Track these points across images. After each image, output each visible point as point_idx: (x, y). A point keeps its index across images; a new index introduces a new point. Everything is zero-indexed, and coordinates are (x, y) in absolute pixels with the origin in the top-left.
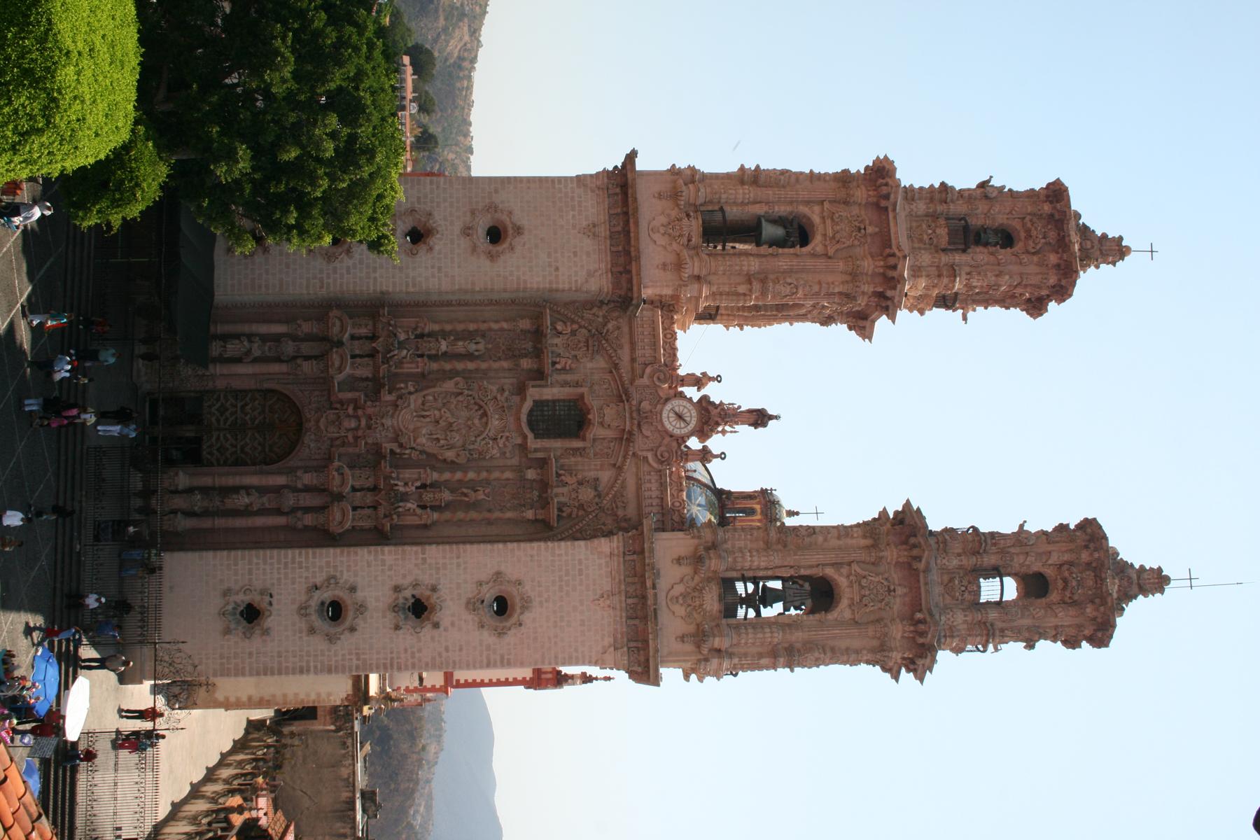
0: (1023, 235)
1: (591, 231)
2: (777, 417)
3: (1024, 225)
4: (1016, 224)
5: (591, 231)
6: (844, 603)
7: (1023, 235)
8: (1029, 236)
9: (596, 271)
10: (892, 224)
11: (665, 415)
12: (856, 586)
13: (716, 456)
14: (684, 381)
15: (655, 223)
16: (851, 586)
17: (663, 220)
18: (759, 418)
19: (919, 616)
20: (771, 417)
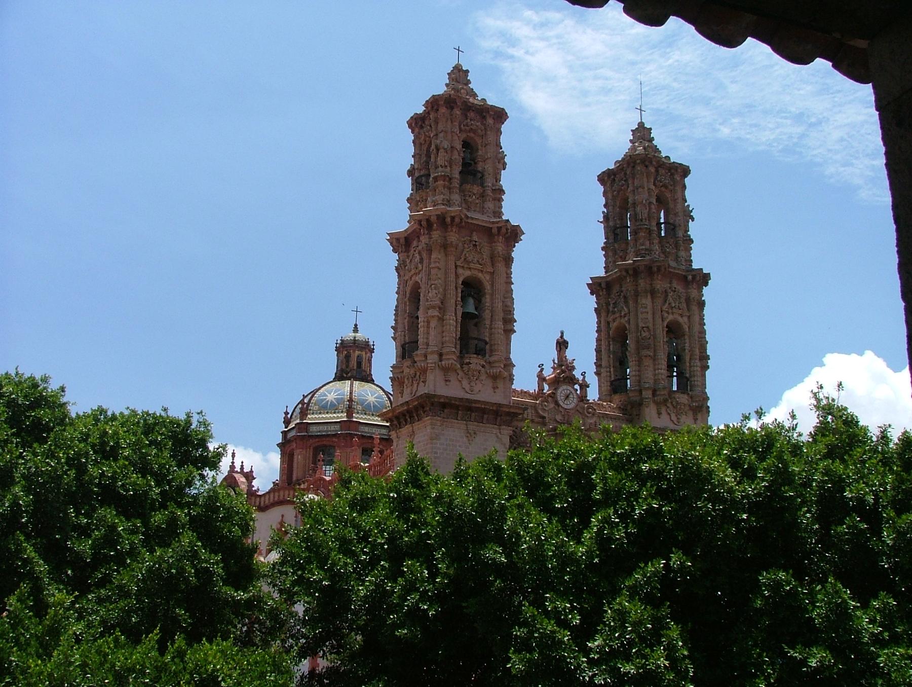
0: (472, 135)
1: (470, 435)
2: (562, 333)
3: (465, 131)
4: (463, 136)
5: (470, 435)
6: (680, 319)
7: (472, 135)
8: (474, 132)
9: (497, 437)
10: (474, 222)
11: (566, 407)
12: (674, 310)
13: (584, 377)
14: (541, 389)
15: (467, 387)
16: (673, 313)
17: (465, 383)
18: (562, 345)
19: (690, 277)
20: (562, 337)
